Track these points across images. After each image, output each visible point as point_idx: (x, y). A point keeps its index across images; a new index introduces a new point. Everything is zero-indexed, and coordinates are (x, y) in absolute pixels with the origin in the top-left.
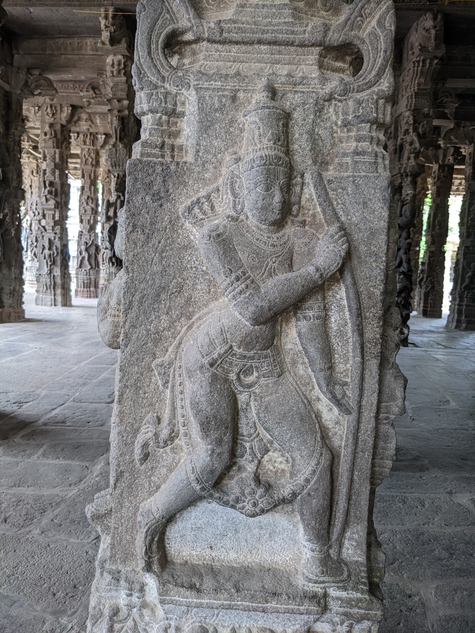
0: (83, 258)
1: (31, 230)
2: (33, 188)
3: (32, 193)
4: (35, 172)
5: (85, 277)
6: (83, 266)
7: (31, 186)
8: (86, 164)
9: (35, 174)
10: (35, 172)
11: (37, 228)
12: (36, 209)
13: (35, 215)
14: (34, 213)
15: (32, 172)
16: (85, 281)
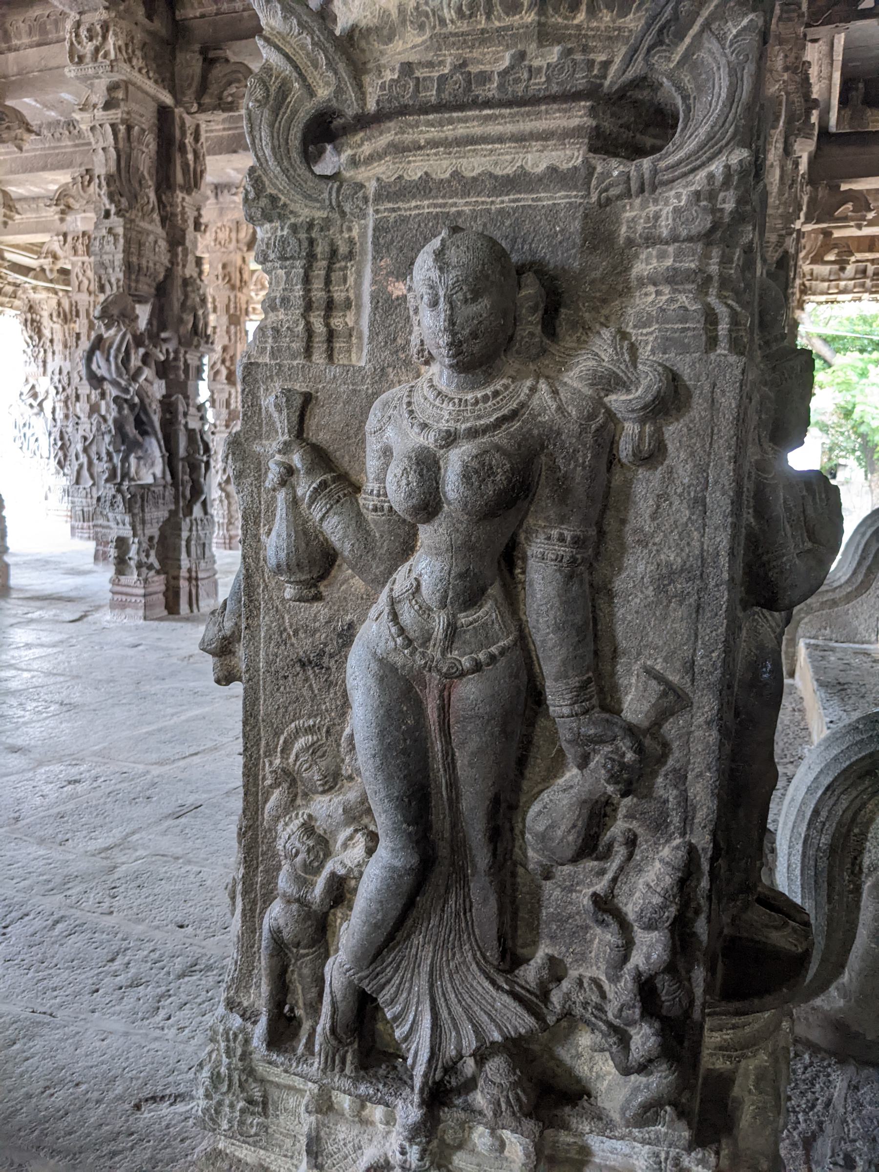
0: (81, 466)
1: (54, 419)
2: (55, 344)
3: (54, 353)
4: (55, 315)
5: (84, 500)
6: (82, 481)
7: (52, 341)
8: (79, 290)
9: (55, 319)
10: (55, 315)
11: (62, 416)
12: (60, 381)
13: (57, 393)
14: (56, 388)
15: (51, 315)
16: (86, 509)
